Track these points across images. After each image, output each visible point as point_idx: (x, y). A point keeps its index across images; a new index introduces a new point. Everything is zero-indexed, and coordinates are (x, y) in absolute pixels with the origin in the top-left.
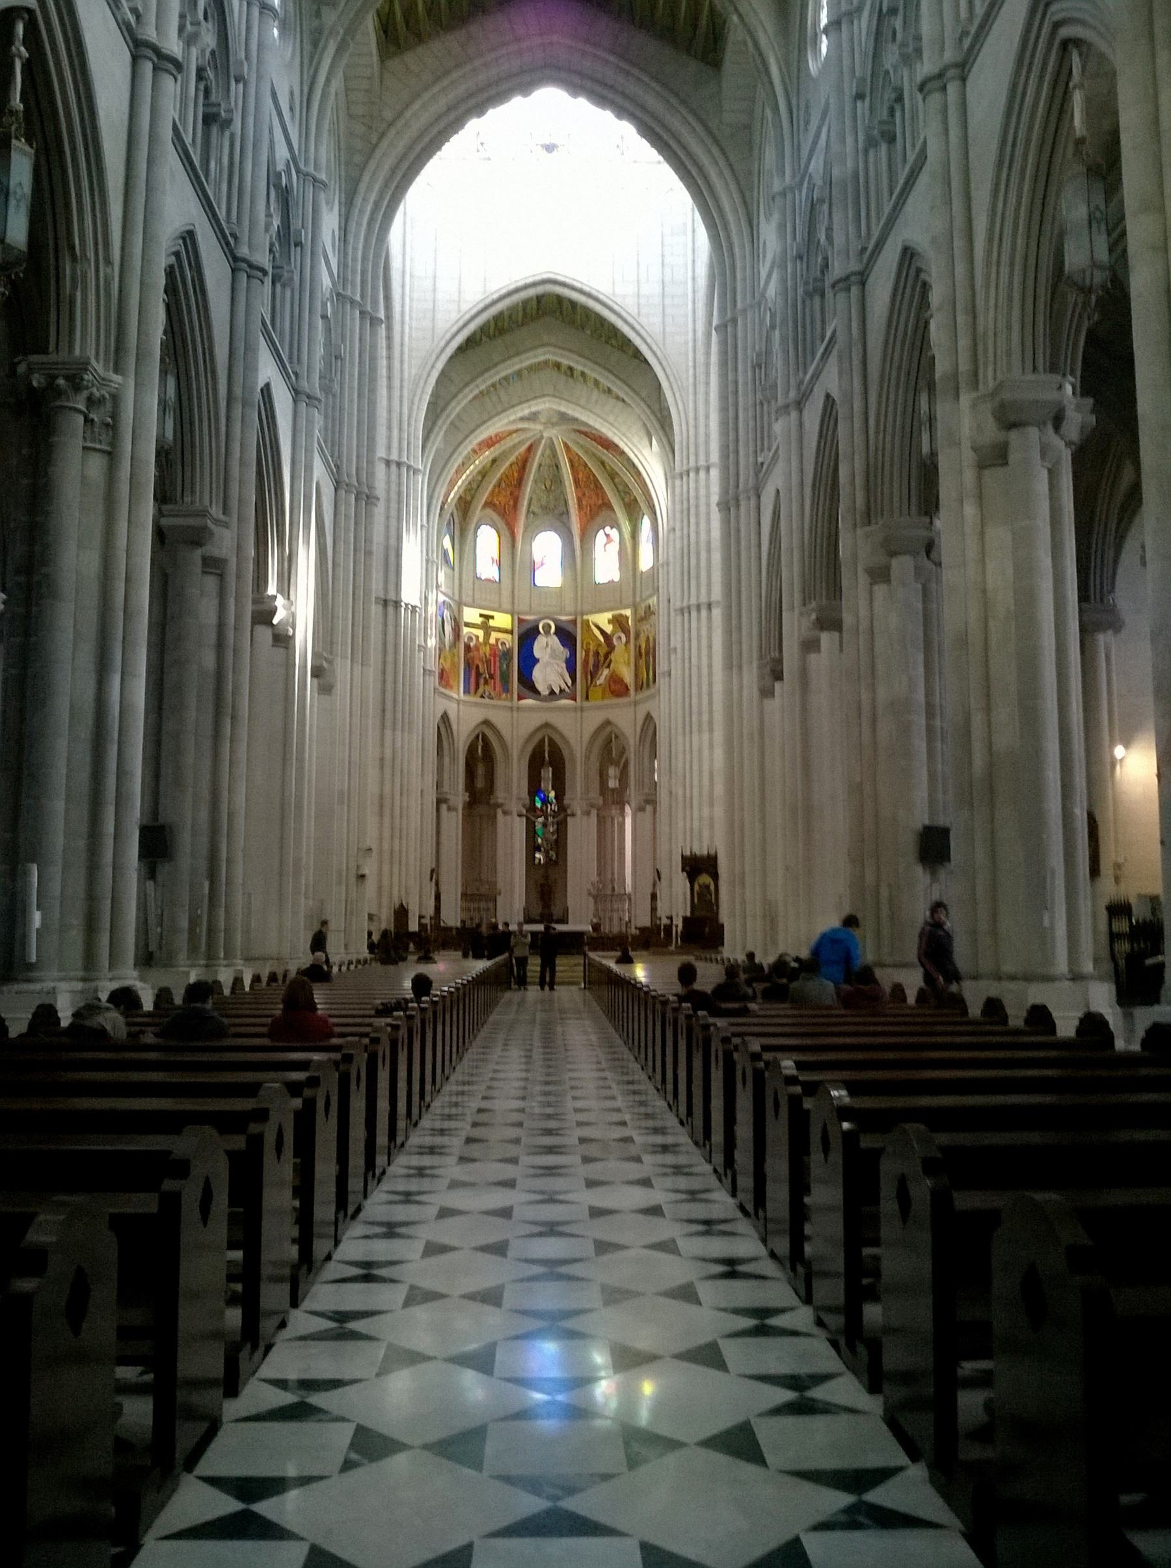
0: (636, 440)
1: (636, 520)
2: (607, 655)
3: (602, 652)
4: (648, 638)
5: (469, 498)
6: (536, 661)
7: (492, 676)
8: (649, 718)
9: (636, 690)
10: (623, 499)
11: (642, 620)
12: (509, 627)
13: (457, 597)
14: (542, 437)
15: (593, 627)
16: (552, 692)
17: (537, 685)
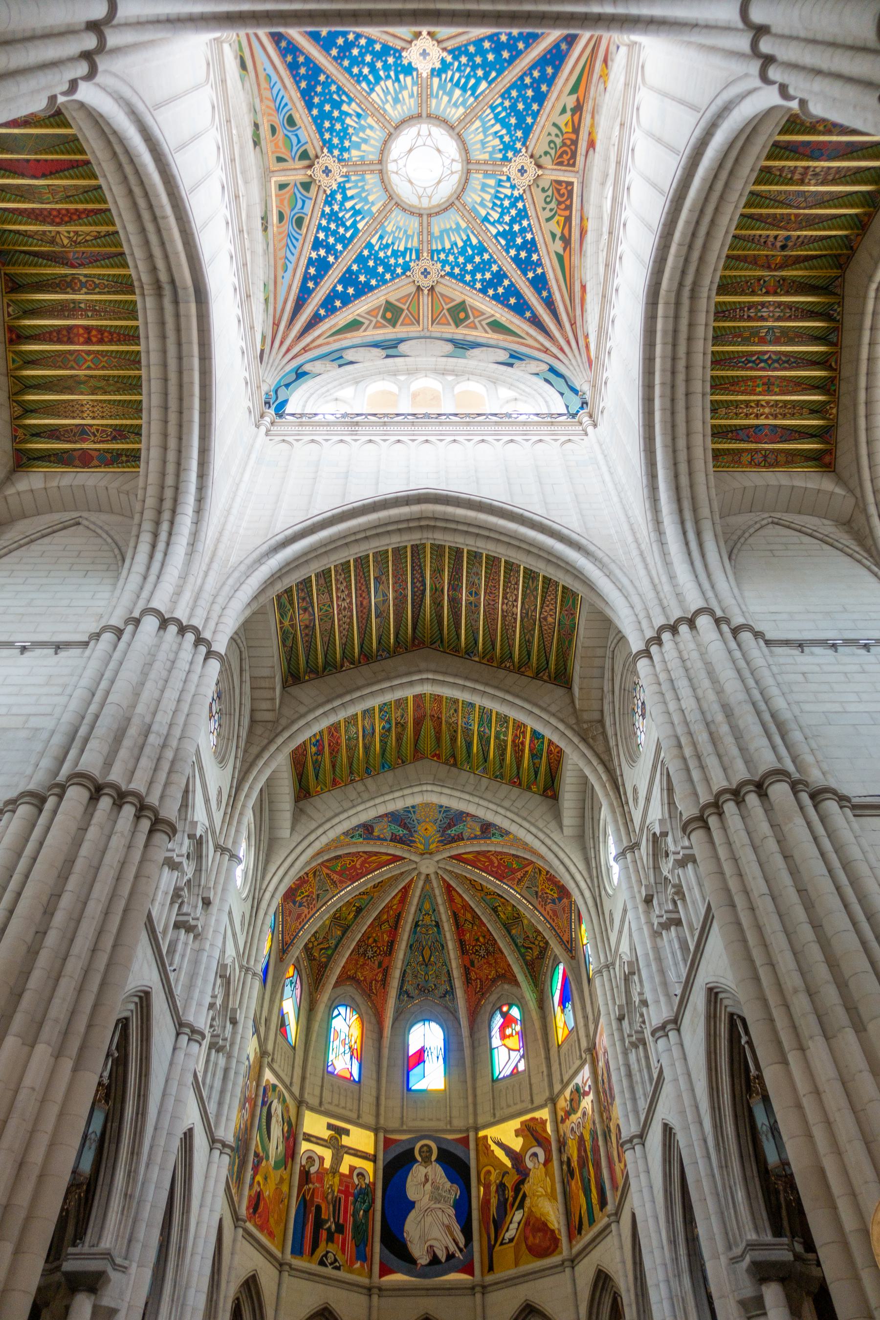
0: (541, 824)
1: (543, 983)
2: (517, 1188)
3: (510, 1182)
4: (581, 1139)
5: (324, 960)
6: (411, 1205)
8: (602, 1279)
9: (570, 1238)
10: (523, 956)
11: (568, 1114)
12: (371, 1150)
13: (296, 1090)
14: (419, 874)
15: (494, 1147)
16: (435, 1261)
17: (409, 1244)
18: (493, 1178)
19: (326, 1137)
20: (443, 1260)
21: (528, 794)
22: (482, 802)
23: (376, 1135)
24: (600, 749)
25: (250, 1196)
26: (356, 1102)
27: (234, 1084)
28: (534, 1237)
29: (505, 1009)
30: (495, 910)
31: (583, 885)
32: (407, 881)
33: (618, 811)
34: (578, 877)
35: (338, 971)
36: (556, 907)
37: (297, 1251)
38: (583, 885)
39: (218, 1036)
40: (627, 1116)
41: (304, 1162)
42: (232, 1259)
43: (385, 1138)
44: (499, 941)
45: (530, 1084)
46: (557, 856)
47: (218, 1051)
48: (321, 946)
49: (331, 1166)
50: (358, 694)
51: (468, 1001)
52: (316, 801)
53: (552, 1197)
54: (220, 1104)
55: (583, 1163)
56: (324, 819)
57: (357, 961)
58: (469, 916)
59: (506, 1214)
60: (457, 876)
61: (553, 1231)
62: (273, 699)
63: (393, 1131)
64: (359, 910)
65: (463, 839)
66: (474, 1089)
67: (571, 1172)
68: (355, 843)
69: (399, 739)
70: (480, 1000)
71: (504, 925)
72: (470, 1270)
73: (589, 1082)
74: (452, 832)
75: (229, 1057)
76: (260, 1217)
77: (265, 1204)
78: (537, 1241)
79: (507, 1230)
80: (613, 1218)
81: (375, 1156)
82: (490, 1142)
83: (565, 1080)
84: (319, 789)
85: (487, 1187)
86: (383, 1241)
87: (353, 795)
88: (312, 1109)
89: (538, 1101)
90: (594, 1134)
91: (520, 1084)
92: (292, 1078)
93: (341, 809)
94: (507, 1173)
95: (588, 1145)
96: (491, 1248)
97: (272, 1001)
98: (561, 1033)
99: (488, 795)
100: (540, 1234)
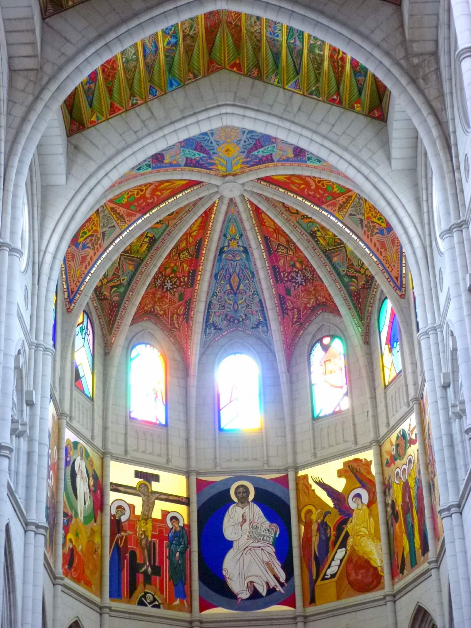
0: (365, 155)
1: (370, 315)
3: (332, 522)
4: (406, 486)
5: (116, 299)
6: (229, 545)
7: (157, 571)
9: (393, 576)
10: (346, 286)
11: (394, 459)
12: (184, 494)
13: (98, 442)
14: (221, 198)
15: (315, 487)
16: (255, 594)
17: (228, 581)
18: (314, 517)
19: (135, 485)
20: (264, 594)
21: (351, 115)
22: (293, 127)
23: (188, 478)
24: (432, 93)
25: (64, 554)
26: (163, 446)
27: (39, 467)
28: (357, 574)
29: (326, 341)
30: (313, 235)
31: (412, 232)
32: (207, 206)
33: (448, 177)
34: (407, 222)
35: (132, 310)
36: (383, 238)
37: (115, 594)
38: (412, 232)
39: (17, 422)
40: (447, 485)
41: (113, 512)
42: (54, 612)
43: (198, 480)
44: (318, 271)
45: (354, 425)
46: (382, 195)
47: (18, 436)
48: (112, 284)
49: (143, 513)
50: (136, 22)
51: (285, 333)
52: (92, 133)
53: (376, 536)
54: (28, 488)
55: (407, 509)
56: (104, 159)
57: (154, 294)
58: (282, 240)
59: (328, 552)
60: (267, 199)
61: (376, 569)
62: (33, 43)
63: (205, 474)
64: (153, 241)
65: (272, 161)
66: (293, 427)
67: (395, 515)
68: (144, 174)
69: (189, 50)
70: (298, 331)
71: (325, 252)
72: (290, 601)
73: (415, 432)
74: (260, 153)
75: (31, 440)
76: (76, 570)
77: (79, 557)
78: (360, 577)
79: (329, 567)
80: (433, 565)
81: (188, 498)
82: (311, 481)
83: (392, 424)
84: (94, 118)
85: (308, 525)
86: (201, 578)
87: (136, 125)
88: (117, 459)
89: (363, 441)
90: (418, 482)
91: (343, 423)
92: (93, 431)
93: (123, 144)
94: (330, 513)
95: (413, 492)
96: (313, 583)
97: (63, 358)
98: (389, 375)
99: (302, 119)
100: (362, 571)
